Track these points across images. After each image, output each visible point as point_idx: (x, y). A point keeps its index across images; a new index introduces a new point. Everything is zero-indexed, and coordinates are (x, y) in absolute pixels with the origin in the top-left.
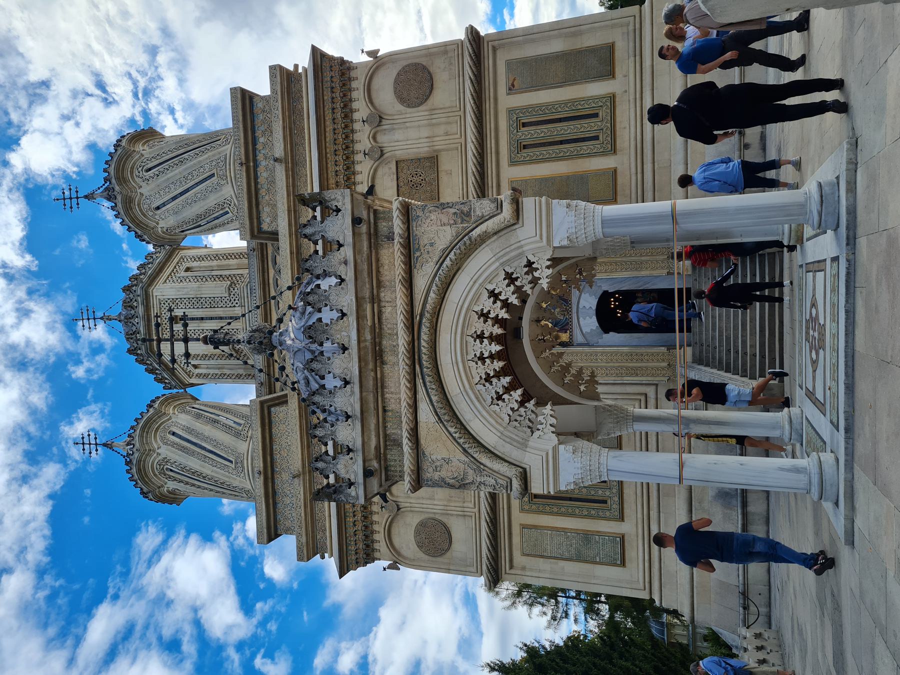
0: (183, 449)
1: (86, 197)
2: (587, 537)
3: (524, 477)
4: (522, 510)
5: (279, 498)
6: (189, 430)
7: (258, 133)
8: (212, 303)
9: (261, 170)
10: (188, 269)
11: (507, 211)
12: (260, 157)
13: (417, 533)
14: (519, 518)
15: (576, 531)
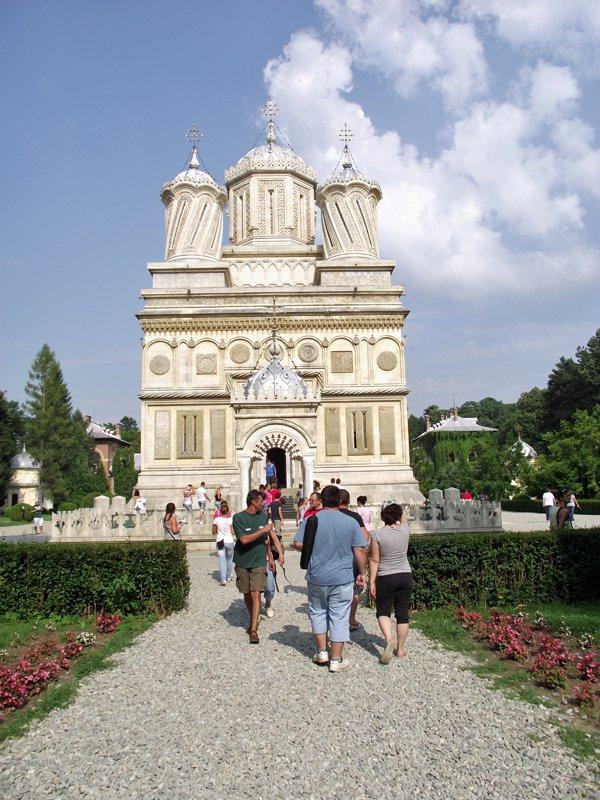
0: (197, 212)
1: (346, 147)
2: (168, 442)
3: (241, 449)
4: (178, 411)
5: (173, 275)
6: (209, 212)
7: (371, 273)
8: (282, 216)
9: (353, 274)
10: (301, 196)
11: (312, 445)
12: (360, 273)
13: (162, 357)
14: (174, 410)
15: (170, 438)
